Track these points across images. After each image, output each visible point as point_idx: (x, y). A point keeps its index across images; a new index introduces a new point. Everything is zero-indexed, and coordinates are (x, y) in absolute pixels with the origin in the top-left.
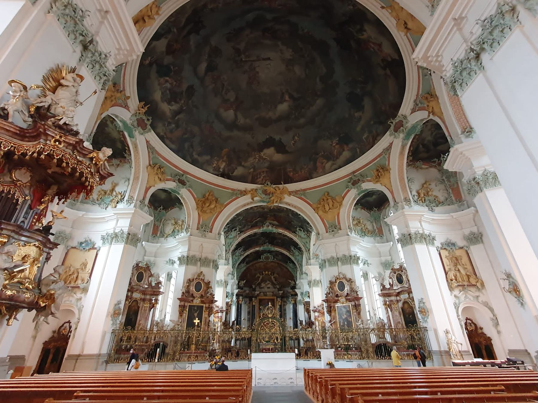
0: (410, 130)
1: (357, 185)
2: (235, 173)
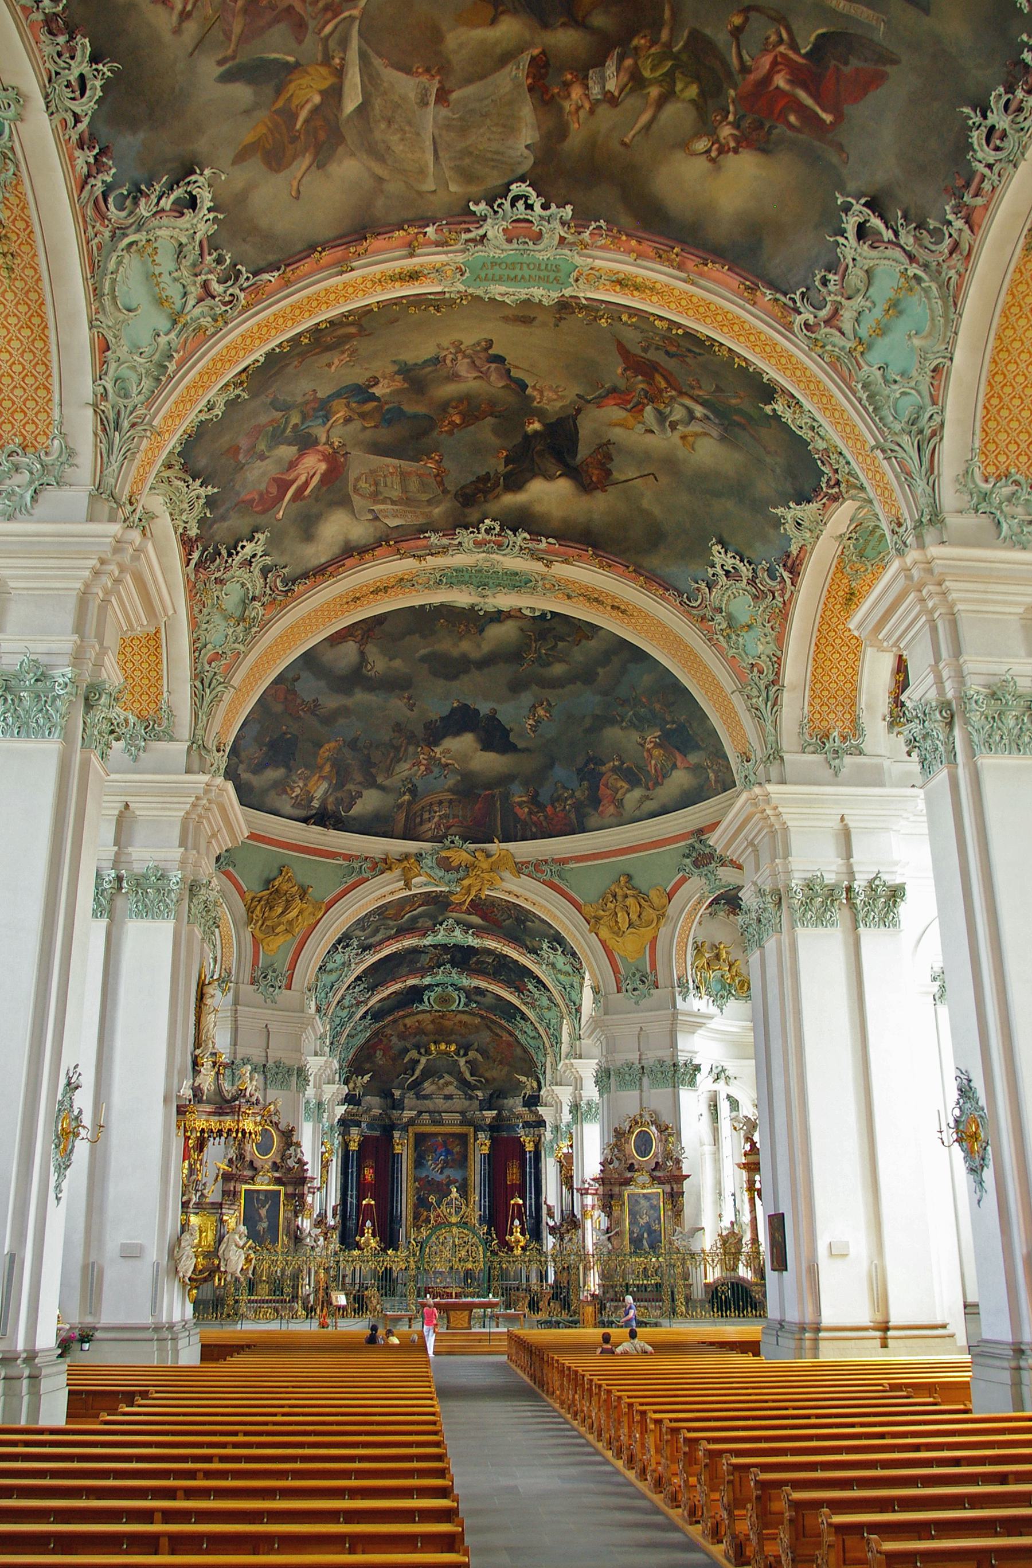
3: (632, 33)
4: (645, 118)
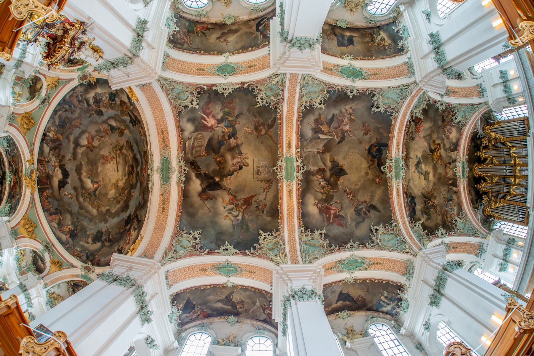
0: (87, 277)
1: (45, 249)
2: (45, 146)
3: (331, 185)
4: (318, 190)
